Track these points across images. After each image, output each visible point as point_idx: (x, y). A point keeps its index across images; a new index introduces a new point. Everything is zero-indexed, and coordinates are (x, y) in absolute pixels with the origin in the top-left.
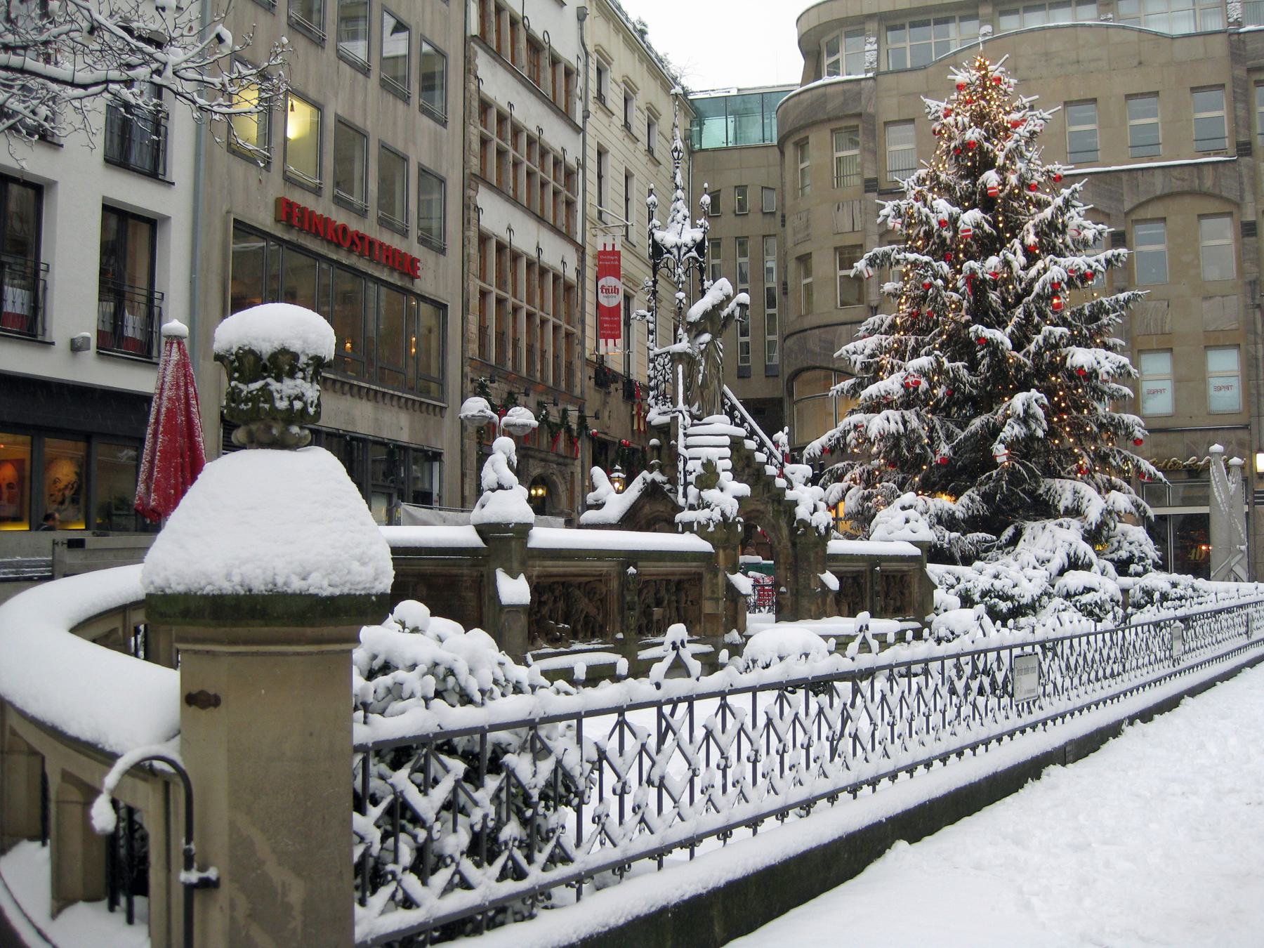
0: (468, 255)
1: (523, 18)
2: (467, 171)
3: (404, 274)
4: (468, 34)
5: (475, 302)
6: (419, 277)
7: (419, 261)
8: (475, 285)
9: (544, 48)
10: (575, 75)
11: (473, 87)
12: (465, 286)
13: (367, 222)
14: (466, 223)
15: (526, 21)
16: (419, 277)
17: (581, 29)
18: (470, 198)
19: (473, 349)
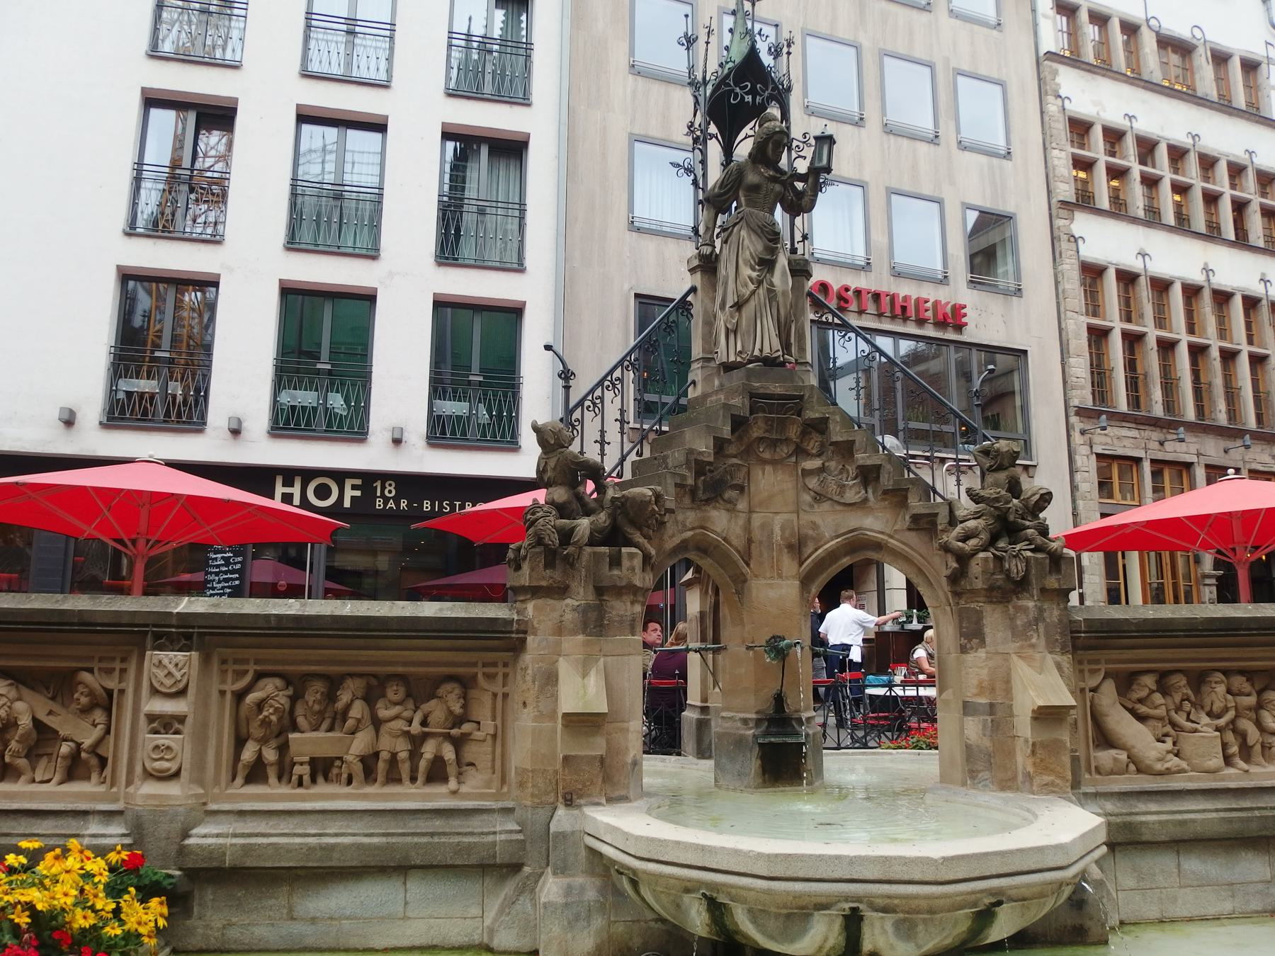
0: (1064, 291)
1: (1148, 21)
2: (1054, 201)
3: (941, 324)
4: (1042, 52)
5: (1080, 342)
6: (966, 324)
7: (965, 307)
8: (1078, 325)
9: (1194, 47)
10: (1264, 66)
11: (1053, 107)
12: (1063, 326)
13: (872, 275)
14: (1056, 257)
15: (1153, 22)
16: (966, 324)
17: (1268, 10)
18: (1059, 228)
19: (1084, 396)
